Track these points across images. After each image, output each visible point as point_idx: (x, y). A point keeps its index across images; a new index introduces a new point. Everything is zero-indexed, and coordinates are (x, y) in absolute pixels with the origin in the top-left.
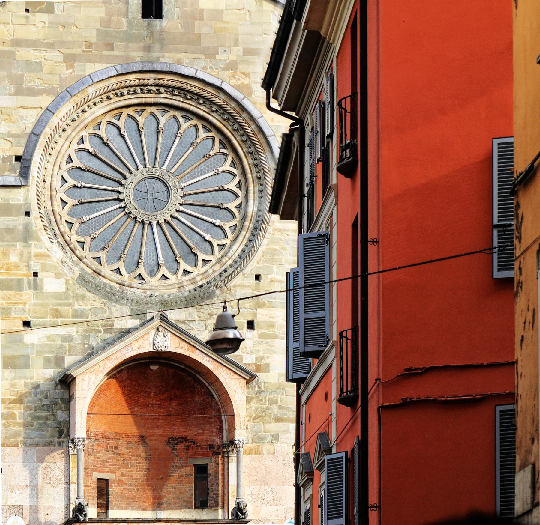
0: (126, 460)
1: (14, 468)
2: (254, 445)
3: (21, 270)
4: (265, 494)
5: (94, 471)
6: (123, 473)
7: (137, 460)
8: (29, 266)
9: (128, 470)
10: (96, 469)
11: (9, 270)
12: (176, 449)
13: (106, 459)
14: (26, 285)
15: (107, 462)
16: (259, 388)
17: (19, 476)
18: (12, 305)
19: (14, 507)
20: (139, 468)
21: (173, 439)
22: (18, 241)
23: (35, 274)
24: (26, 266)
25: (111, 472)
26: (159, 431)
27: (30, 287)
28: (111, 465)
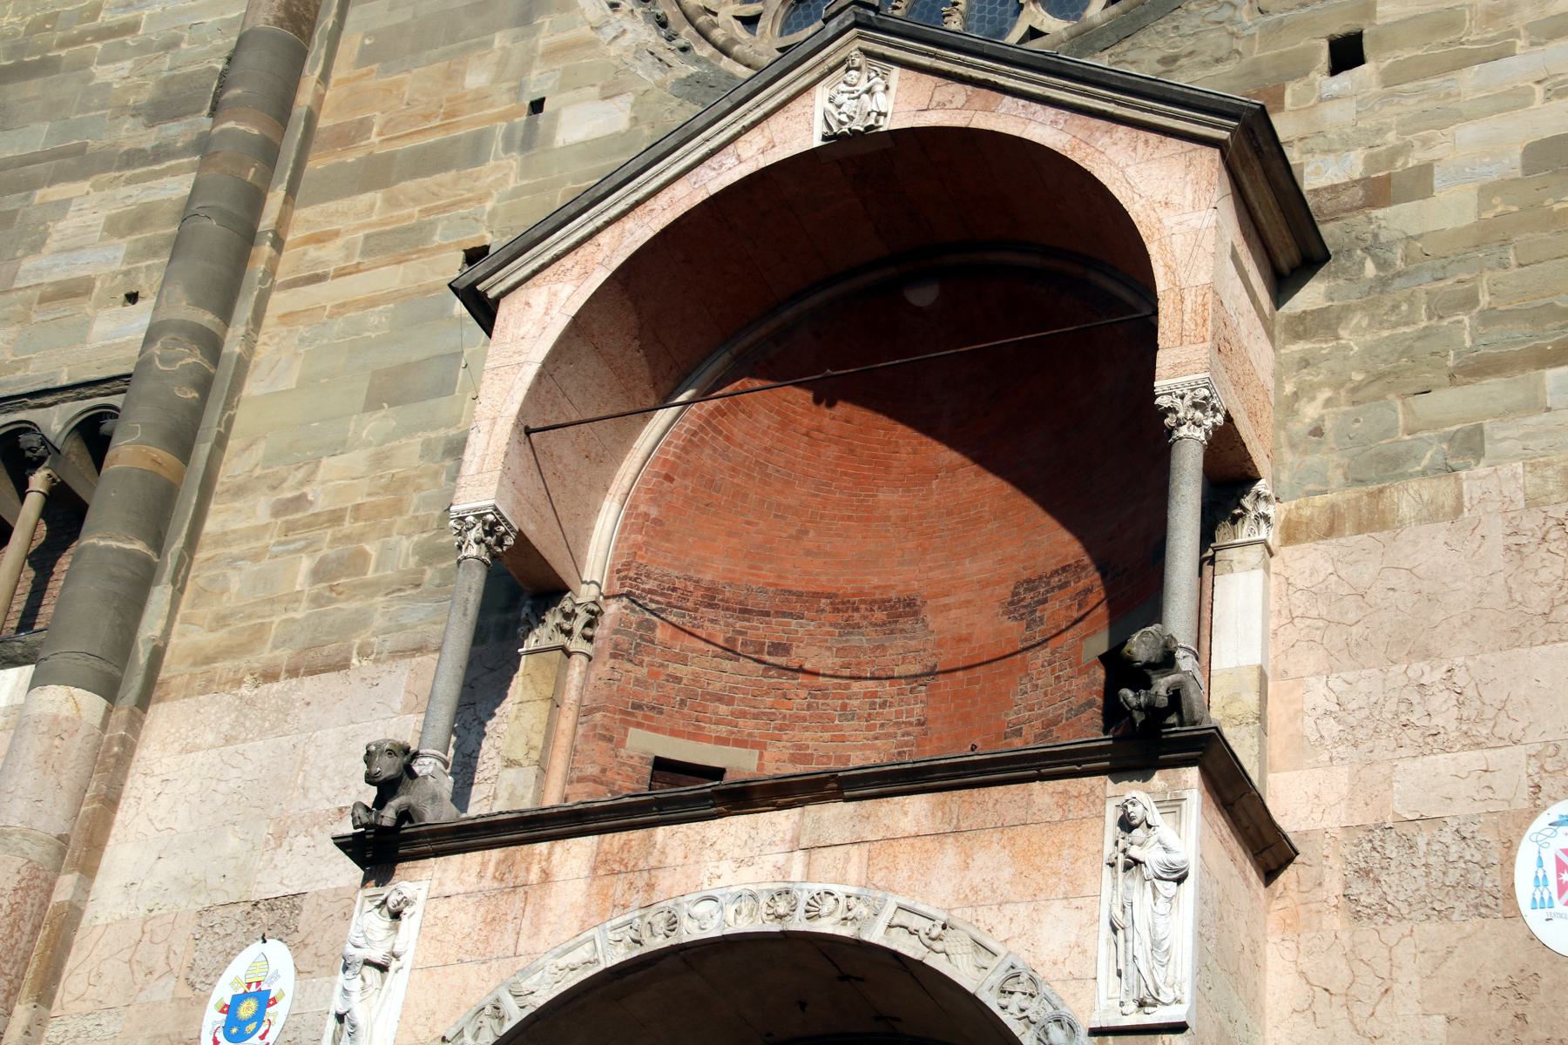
0: (825, 696)
1: (311, 751)
2: (1351, 493)
3: (491, 106)
4: (1415, 698)
5: (639, 725)
6: (800, 747)
7: (874, 694)
8: (518, 90)
9: (827, 735)
10: (646, 717)
11: (454, 116)
12: (1041, 618)
13: (716, 687)
14: (497, 144)
15: (720, 699)
16: (1382, 265)
17: (324, 776)
18: (437, 214)
19: (271, 904)
20: (882, 725)
21: (1030, 584)
22: (499, 28)
23: (537, 106)
24: (510, 90)
25: (740, 743)
26: (973, 569)
27: (508, 148)
28: (743, 715)
